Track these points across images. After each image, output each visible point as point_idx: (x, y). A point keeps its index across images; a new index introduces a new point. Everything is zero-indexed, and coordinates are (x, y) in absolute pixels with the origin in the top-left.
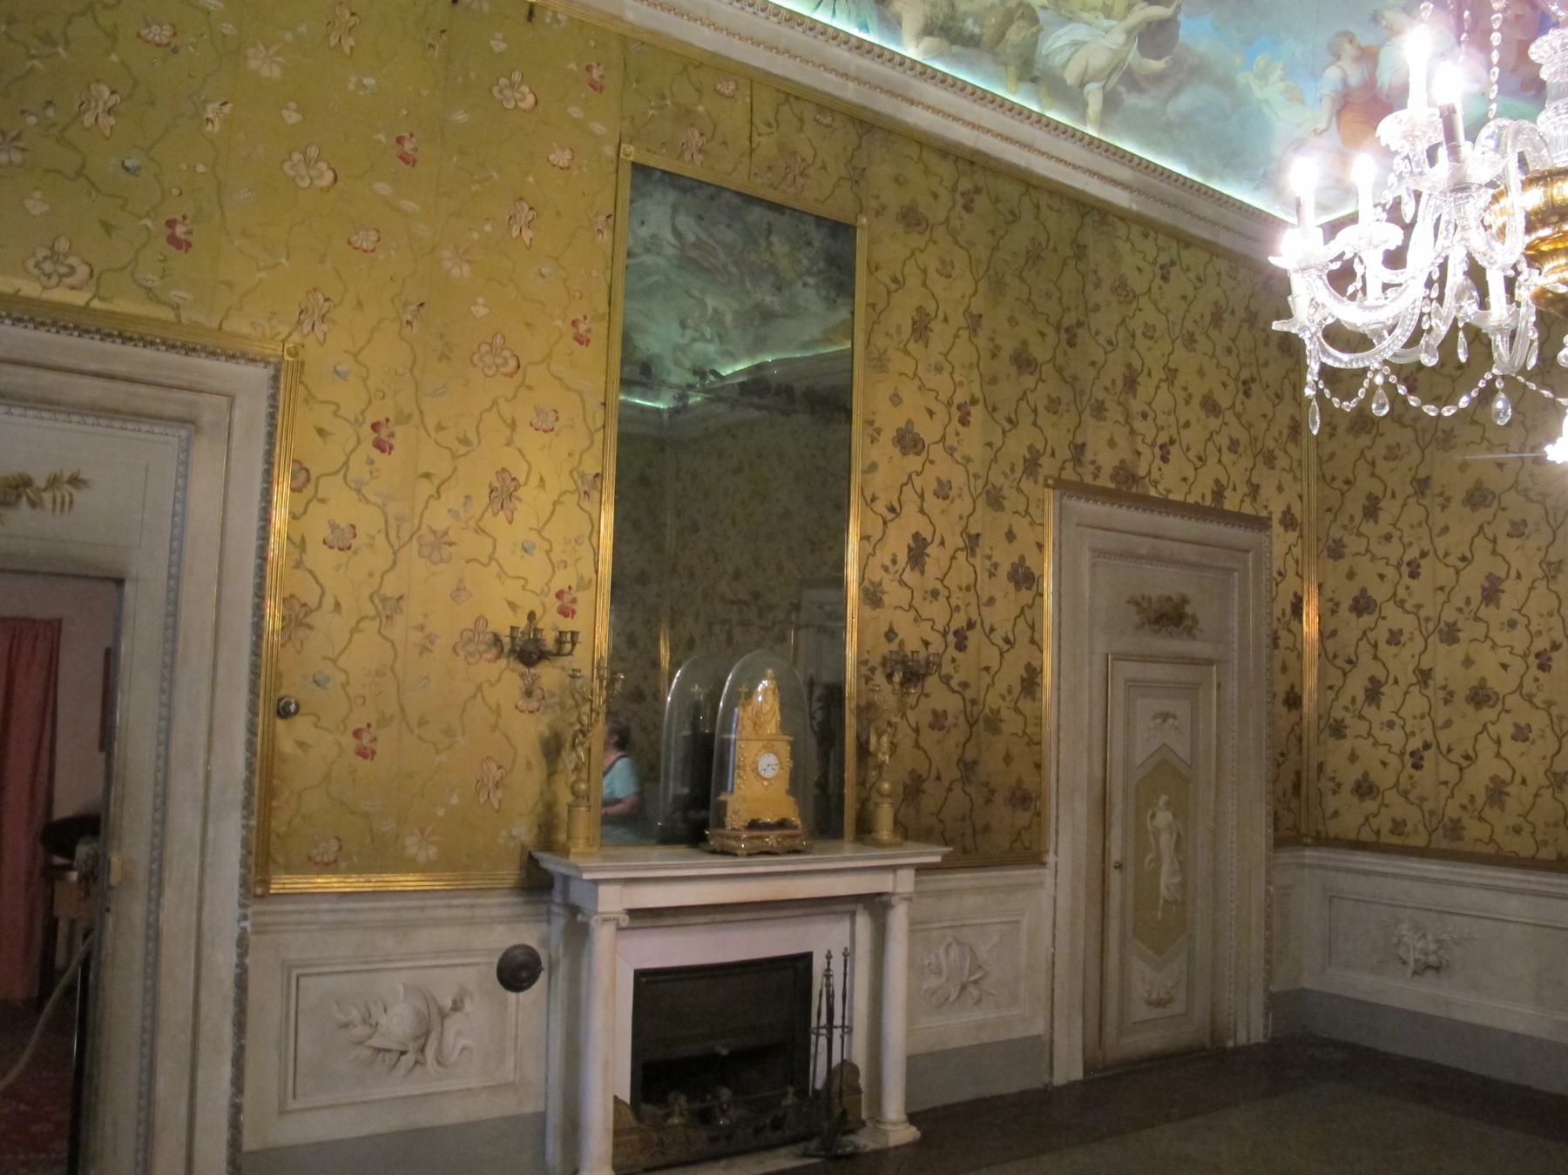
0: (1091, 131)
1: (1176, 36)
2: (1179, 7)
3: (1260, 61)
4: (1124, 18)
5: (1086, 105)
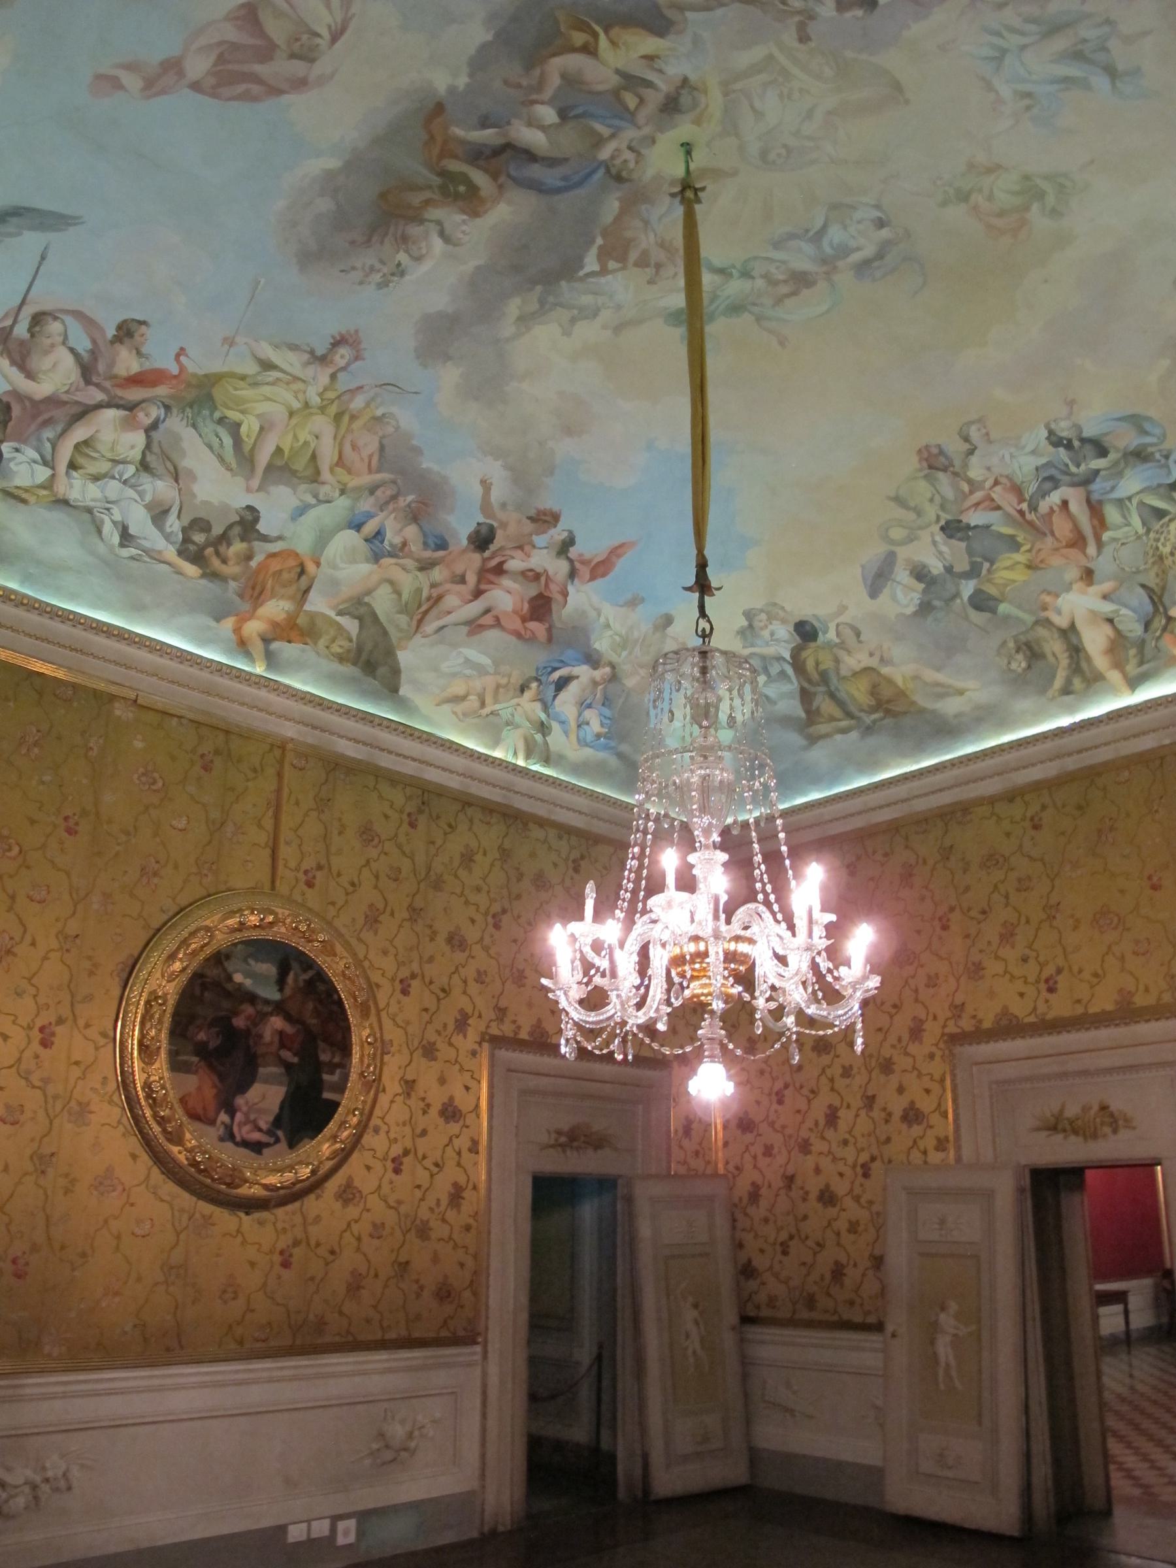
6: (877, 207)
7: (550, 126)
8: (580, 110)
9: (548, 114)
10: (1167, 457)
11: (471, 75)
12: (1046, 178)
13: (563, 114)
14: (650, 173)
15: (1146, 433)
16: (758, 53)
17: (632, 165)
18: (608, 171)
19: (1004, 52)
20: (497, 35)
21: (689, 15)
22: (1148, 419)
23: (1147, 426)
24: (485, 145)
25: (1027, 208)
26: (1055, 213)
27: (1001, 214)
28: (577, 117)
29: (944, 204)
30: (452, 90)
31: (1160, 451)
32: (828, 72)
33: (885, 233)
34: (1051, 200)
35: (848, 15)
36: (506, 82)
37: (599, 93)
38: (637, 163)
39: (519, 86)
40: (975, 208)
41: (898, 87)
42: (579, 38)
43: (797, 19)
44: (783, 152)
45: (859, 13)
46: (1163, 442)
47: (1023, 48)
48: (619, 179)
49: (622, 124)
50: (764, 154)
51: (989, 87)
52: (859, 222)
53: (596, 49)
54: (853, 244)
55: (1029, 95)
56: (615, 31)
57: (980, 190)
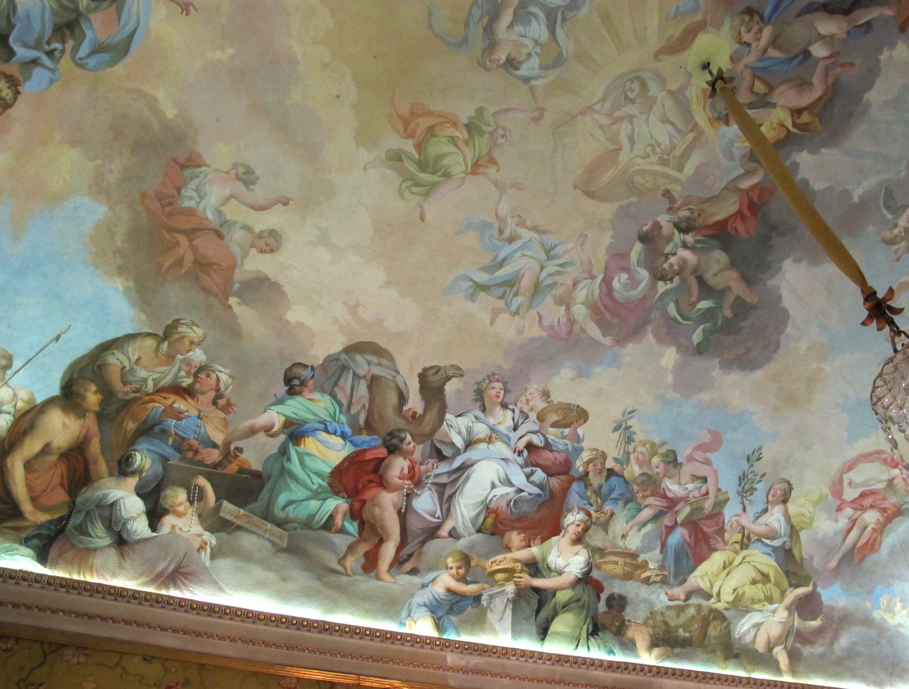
0: (787, 678)
1: (821, 602)
2: (815, 586)
3: (884, 601)
4: (782, 601)
5: (777, 663)
6: (527, 80)
7: (816, 41)
8: (796, 61)
9: (819, 51)
10: (50, 54)
11: (879, 61)
12: (434, 185)
13: (807, 54)
14: (727, 26)
15: (97, 50)
16: (690, 167)
17: (743, 29)
18: (762, 17)
19: (549, 258)
20: (861, 98)
21: (741, 171)
22: (113, 63)
23: (105, 57)
24: (866, 7)
25: (419, 147)
26: (395, 158)
27: (431, 131)
28: (796, 57)
29: (480, 112)
30: (892, 46)
31: (63, 52)
32: (638, 179)
33: (501, 56)
34: (412, 168)
35: (650, 223)
36: (852, 64)
37: (783, 83)
38: (740, 33)
39: (842, 66)
40: (455, 124)
41: (591, 195)
42: (805, 118)
43: (678, 203)
44: (631, 95)
45: (645, 228)
46: (73, 58)
47: (542, 268)
48: (750, 11)
49: (758, 65)
50: (644, 84)
51: (535, 229)
52: (529, 55)
53: (792, 116)
54: (519, 29)
55: (511, 240)
56: (783, 134)
57: (466, 143)
